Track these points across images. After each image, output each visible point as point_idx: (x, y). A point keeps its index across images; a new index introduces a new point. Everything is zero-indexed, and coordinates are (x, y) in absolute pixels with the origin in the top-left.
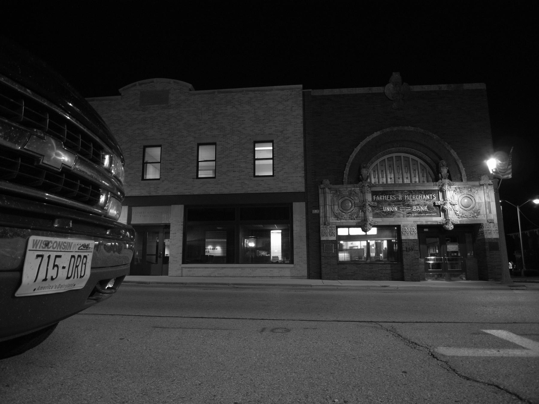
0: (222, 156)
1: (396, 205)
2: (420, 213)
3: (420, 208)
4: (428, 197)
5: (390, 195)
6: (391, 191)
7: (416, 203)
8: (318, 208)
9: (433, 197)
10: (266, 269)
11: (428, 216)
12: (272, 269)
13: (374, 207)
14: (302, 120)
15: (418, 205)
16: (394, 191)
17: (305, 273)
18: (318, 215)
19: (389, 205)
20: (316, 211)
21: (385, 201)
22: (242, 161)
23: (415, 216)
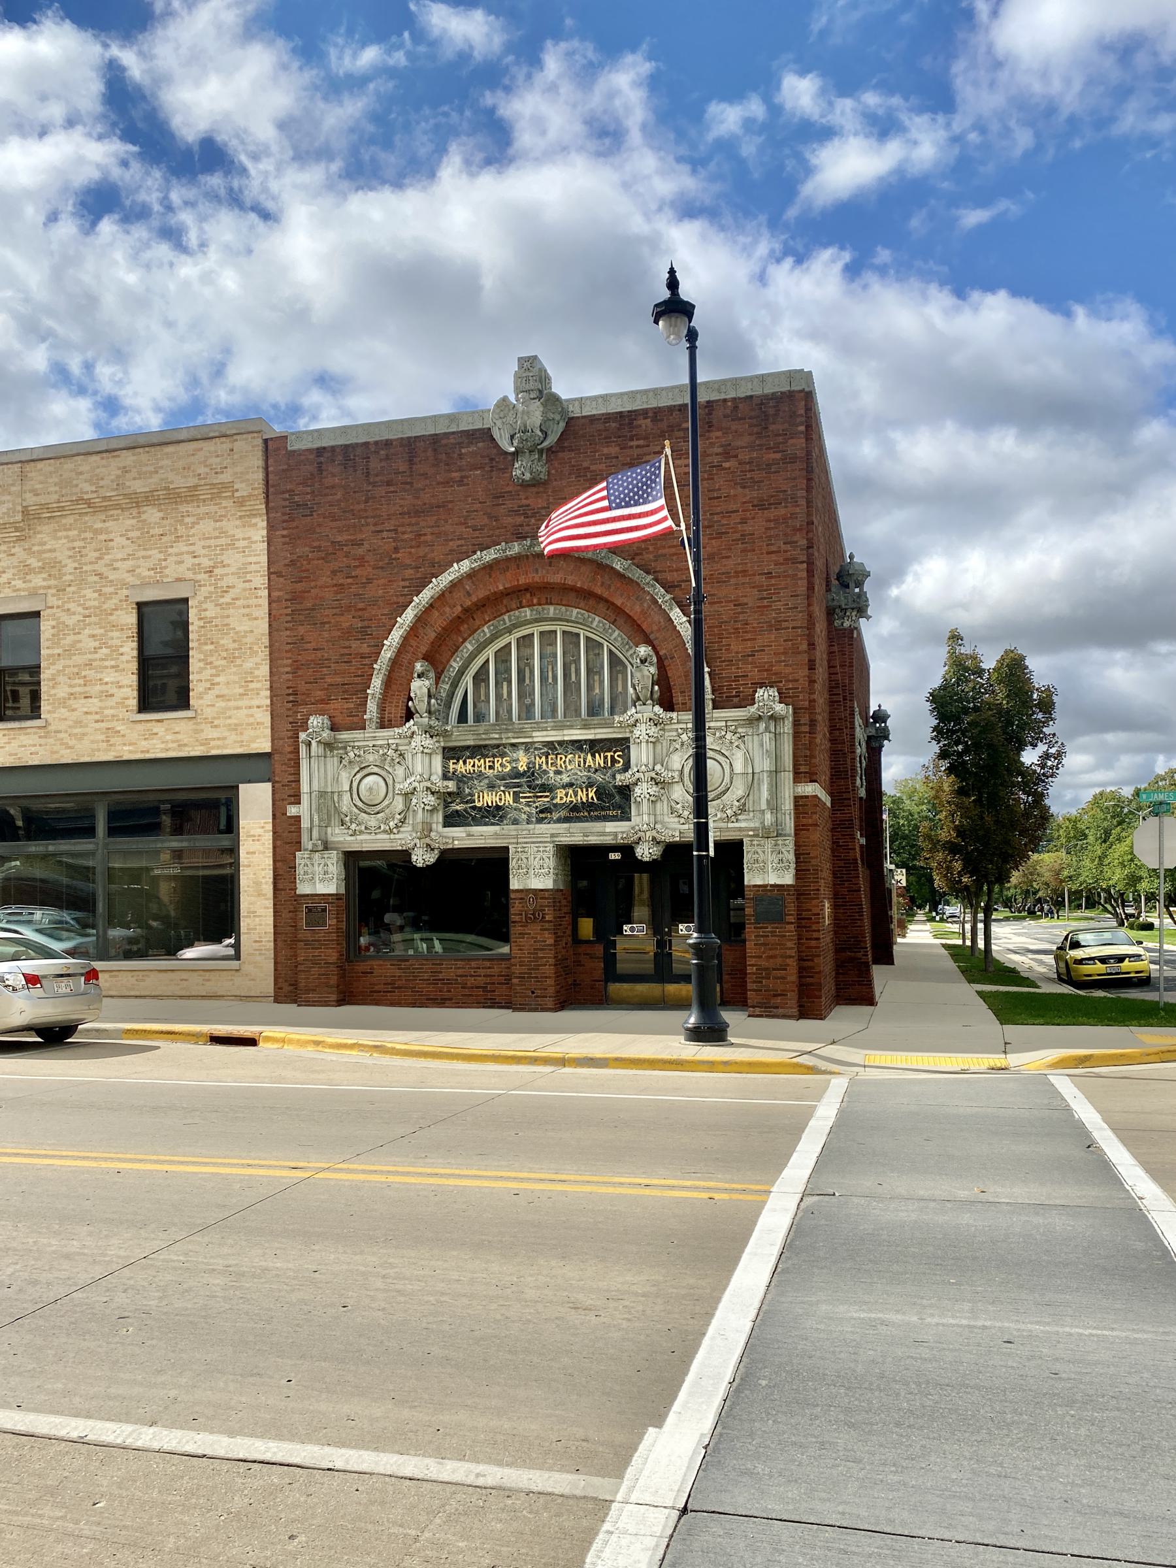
0: (57, 651)
1: (507, 786)
2: (574, 808)
3: (576, 796)
5: (494, 756)
6: (498, 746)
7: (566, 779)
9: (614, 761)
10: (170, 974)
12: (184, 975)
13: (450, 794)
14: (265, 532)
15: (571, 785)
16: (504, 745)
18: (298, 819)
19: (491, 787)
20: (292, 811)
21: (481, 774)
22: (106, 663)
23: (559, 821)
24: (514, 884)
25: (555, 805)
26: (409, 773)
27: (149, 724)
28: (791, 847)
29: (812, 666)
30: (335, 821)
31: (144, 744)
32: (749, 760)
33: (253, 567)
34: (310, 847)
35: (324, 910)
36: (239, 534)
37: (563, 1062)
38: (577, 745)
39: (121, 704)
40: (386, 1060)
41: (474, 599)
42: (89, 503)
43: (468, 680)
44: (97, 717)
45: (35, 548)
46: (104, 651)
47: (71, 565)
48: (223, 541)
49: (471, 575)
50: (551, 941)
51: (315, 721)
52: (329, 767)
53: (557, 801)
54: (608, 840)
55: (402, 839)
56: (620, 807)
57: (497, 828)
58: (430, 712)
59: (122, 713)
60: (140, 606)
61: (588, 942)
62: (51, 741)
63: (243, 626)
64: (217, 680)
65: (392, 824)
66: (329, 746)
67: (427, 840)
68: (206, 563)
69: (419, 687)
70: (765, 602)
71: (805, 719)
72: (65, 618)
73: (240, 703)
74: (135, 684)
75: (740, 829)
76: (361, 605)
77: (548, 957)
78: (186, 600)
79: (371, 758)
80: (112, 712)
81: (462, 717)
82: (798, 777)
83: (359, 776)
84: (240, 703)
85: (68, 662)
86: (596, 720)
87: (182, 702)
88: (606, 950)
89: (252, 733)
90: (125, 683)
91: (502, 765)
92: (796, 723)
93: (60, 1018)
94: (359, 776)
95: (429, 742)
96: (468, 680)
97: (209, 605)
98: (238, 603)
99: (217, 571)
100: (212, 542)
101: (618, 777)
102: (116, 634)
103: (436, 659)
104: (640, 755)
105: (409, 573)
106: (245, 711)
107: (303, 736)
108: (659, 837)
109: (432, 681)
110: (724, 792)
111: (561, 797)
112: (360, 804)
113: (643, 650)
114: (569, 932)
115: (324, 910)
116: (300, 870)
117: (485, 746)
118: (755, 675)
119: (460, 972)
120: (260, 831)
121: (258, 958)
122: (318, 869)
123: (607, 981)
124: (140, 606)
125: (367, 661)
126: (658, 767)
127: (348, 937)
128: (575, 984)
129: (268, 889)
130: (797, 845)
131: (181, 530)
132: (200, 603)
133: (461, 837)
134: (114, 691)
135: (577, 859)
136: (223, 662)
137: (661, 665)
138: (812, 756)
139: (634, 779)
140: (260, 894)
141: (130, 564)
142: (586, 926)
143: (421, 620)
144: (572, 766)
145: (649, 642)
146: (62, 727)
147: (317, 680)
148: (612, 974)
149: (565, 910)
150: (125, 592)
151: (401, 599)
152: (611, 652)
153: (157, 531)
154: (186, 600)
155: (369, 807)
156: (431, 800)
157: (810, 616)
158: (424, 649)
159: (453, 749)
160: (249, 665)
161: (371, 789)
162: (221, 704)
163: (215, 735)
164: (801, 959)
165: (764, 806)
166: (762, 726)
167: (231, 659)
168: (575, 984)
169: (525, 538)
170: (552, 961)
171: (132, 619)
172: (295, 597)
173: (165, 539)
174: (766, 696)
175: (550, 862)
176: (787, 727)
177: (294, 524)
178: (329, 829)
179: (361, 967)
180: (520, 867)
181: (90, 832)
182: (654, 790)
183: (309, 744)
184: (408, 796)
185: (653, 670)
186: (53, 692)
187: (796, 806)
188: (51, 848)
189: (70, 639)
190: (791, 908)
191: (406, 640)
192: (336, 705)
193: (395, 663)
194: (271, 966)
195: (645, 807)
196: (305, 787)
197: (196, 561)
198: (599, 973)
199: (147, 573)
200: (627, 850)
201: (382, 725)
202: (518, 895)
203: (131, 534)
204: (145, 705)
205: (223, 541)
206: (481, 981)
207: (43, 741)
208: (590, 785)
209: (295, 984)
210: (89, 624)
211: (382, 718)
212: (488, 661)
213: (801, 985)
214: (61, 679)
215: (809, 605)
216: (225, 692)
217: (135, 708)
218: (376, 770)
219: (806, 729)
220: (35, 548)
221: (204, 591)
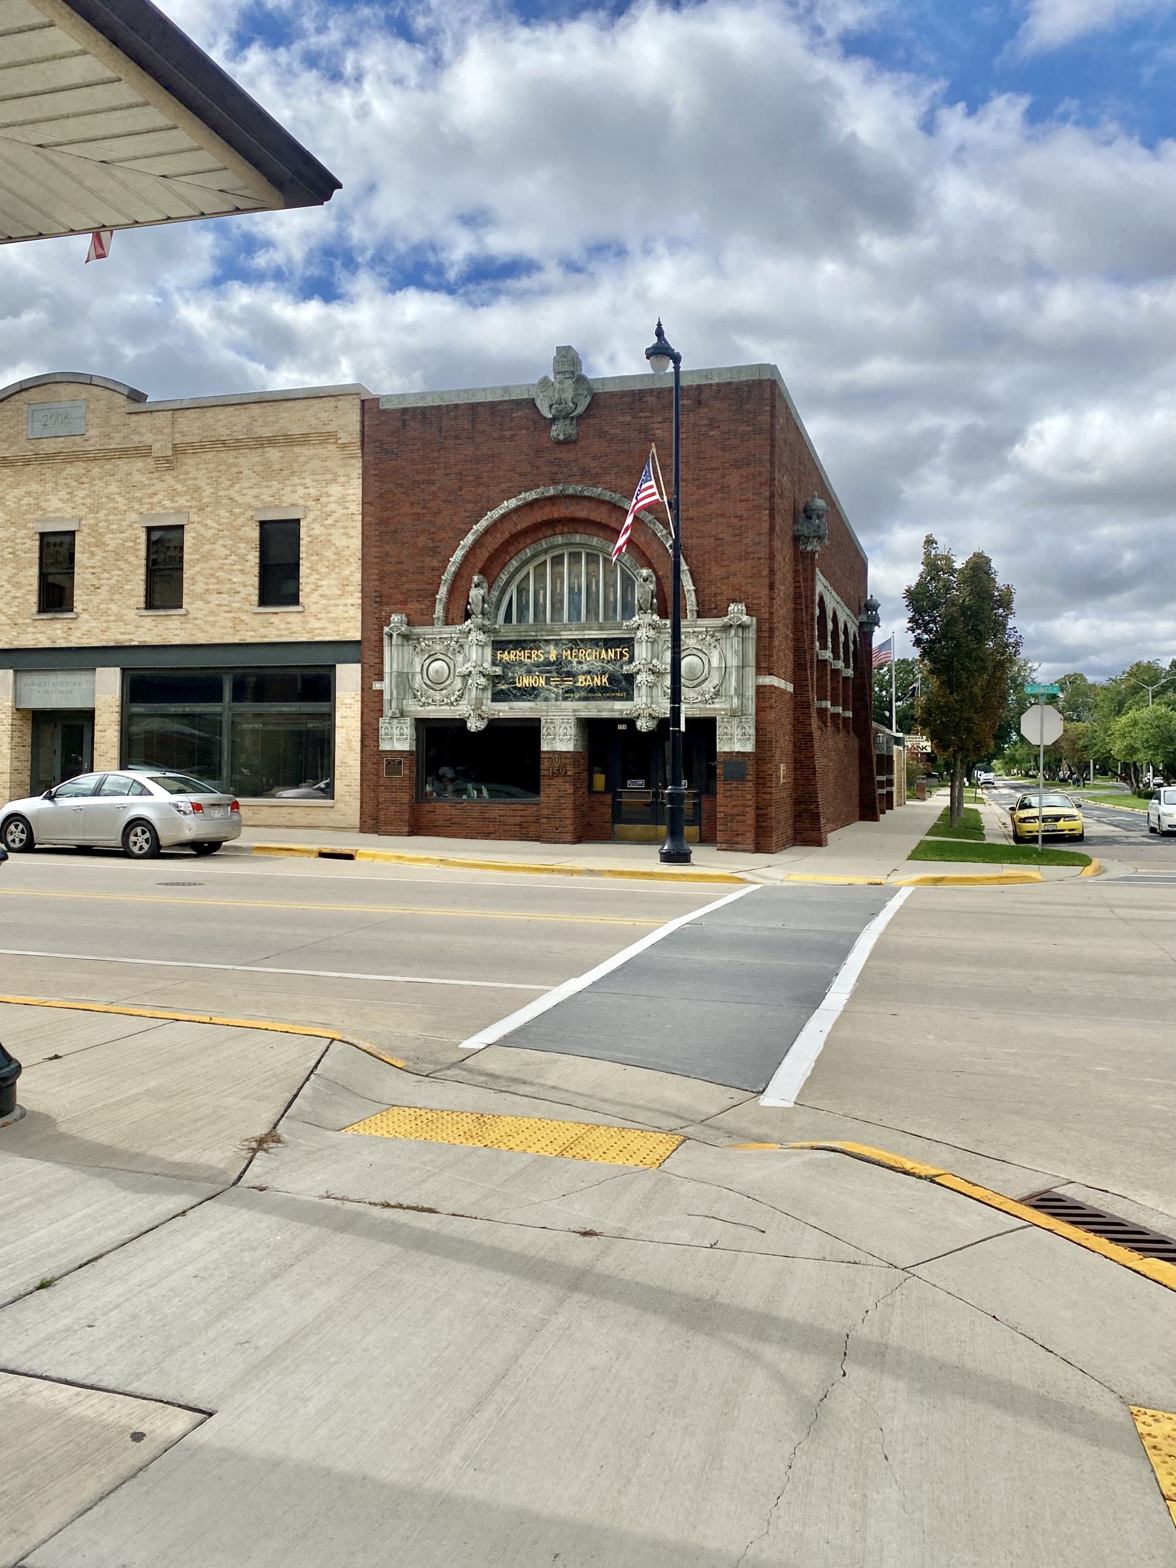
2: (592, 690)
4: (611, 654)
5: (531, 649)
6: (534, 641)
7: (585, 667)
8: (381, 679)
9: (622, 655)
11: (609, 698)
13: (497, 676)
14: (360, 471)
15: (589, 672)
16: (539, 641)
17: (355, 819)
19: (529, 672)
20: (377, 686)
23: (580, 699)
24: (544, 747)
25: (577, 687)
26: (467, 660)
27: (267, 616)
28: (752, 723)
29: (772, 587)
30: (411, 696)
31: (263, 631)
32: (723, 657)
33: (350, 498)
34: (390, 715)
35: (400, 763)
36: (341, 471)
37: (572, 872)
38: (595, 642)
39: (246, 599)
40: (448, 869)
41: (519, 528)
42: (224, 442)
43: (513, 589)
44: (227, 609)
45: (181, 477)
46: (233, 557)
47: (208, 490)
48: (328, 476)
49: (517, 510)
50: (571, 791)
51: (395, 618)
52: (406, 654)
53: (579, 684)
54: (616, 715)
55: (462, 710)
56: (626, 690)
57: (531, 704)
58: (483, 613)
59: (247, 607)
60: (262, 524)
61: (600, 792)
62: (190, 626)
63: (341, 542)
64: (321, 583)
65: (453, 699)
66: (406, 637)
67: (479, 712)
68: (313, 492)
69: (475, 594)
70: (738, 538)
71: (766, 627)
72: (202, 530)
73: (339, 602)
74: (257, 584)
75: (715, 709)
76: (433, 530)
77: (568, 802)
78: (298, 521)
79: (438, 648)
80: (237, 605)
81: (508, 618)
82: (759, 671)
83: (428, 662)
84: (339, 602)
85: (204, 565)
86: (609, 623)
87: (293, 599)
88: (613, 799)
89: (347, 625)
90: (249, 581)
91: (538, 656)
92: (759, 631)
93: (205, 836)
94: (428, 662)
95: (482, 637)
96: (513, 589)
97: (316, 526)
98: (339, 525)
99: (322, 500)
100: (318, 477)
101: (625, 668)
102: (242, 545)
103: (489, 571)
104: (642, 652)
105: (470, 506)
106: (341, 608)
107: (386, 629)
108: (655, 714)
109: (486, 590)
110: (704, 681)
111: (582, 681)
112: (428, 682)
113: (645, 572)
114: (585, 785)
115: (400, 763)
116: (382, 732)
117: (525, 641)
118: (728, 593)
119: (501, 813)
120: (352, 701)
121: (348, 798)
122: (396, 732)
123: (614, 822)
124: (262, 524)
125: (437, 573)
126: (654, 661)
127: (417, 785)
128: (589, 824)
129: (357, 745)
130: (758, 723)
131: (296, 467)
132: (309, 523)
133: (505, 710)
134: (240, 588)
135: (590, 728)
136: (326, 570)
137: (659, 583)
138: (771, 656)
139: (635, 670)
140: (351, 749)
141: (254, 492)
142: (600, 781)
143: (477, 543)
144: (590, 658)
145: (650, 565)
146: (199, 615)
147: (398, 585)
148: (618, 815)
149: (582, 768)
150: (252, 513)
151: (463, 526)
152: (622, 570)
153: (277, 467)
154: (298, 521)
155: (437, 684)
156: (482, 681)
157: (771, 548)
158: (480, 565)
159: (501, 642)
160: (346, 572)
161: (437, 672)
162: (324, 602)
163: (318, 625)
164: (758, 808)
165: (732, 693)
166: (733, 632)
167: (332, 567)
168: (589, 824)
169: (558, 483)
170: (571, 806)
171: (255, 534)
172: (383, 522)
173: (283, 473)
174: (737, 611)
175: (572, 731)
176: (752, 634)
177: (382, 466)
178: (405, 702)
179: (427, 807)
180: (549, 734)
181: (219, 699)
182: (651, 678)
183: (391, 636)
184: (466, 677)
185: (652, 587)
186: (192, 588)
187: (757, 693)
188: (187, 709)
189: (207, 548)
190: (751, 770)
191: (466, 558)
192: (413, 606)
193: (457, 575)
194: (357, 804)
195: (644, 690)
196: (387, 669)
197: (307, 491)
198: (608, 817)
199: (268, 499)
200: (631, 722)
201: (447, 622)
202: (547, 756)
203: (256, 469)
204: (264, 601)
205: (328, 476)
206: (518, 820)
207: (184, 626)
208: (604, 673)
209: (376, 819)
210: (223, 537)
211: (446, 617)
212: (527, 576)
213: (758, 827)
214: (199, 578)
215: (770, 541)
216: (327, 592)
217: (256, 603)
218: (441, 657)
219: (766, 634)
220: (181, 477)
221: (311, 516)
